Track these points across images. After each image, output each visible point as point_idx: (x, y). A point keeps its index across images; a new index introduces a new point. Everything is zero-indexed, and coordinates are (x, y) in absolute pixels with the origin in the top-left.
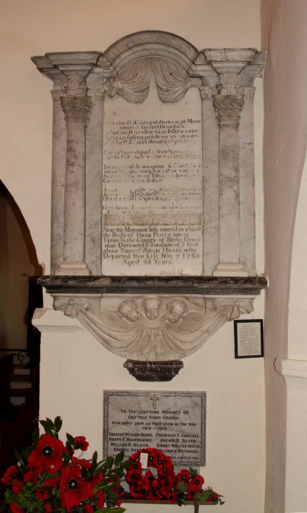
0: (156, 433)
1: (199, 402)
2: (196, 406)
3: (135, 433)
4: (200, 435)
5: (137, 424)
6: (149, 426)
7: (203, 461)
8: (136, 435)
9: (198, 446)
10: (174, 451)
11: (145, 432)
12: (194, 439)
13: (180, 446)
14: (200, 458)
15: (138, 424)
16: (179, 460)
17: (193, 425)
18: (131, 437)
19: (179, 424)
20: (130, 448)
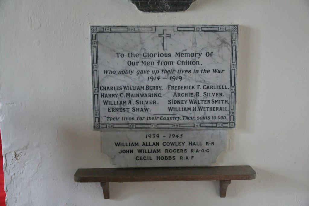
0: (167, 85)
1: (229, 40)
2: (223, 45)
3: (137, 86)
4: (228, 87)
5: (140, 72)
6: (157, 75)
7: (232, 121)
8: (139, 88)
9: (226, 102)
10: (192, 109)
11: (152, 84)
12: (220, 91)
13: (200, 102)
14: (228, 117)
15: (142, 72)
16: (200, 121)
17: (219, 72)
18: (131, 92)
19: (200, 72)
20: (130, 106)
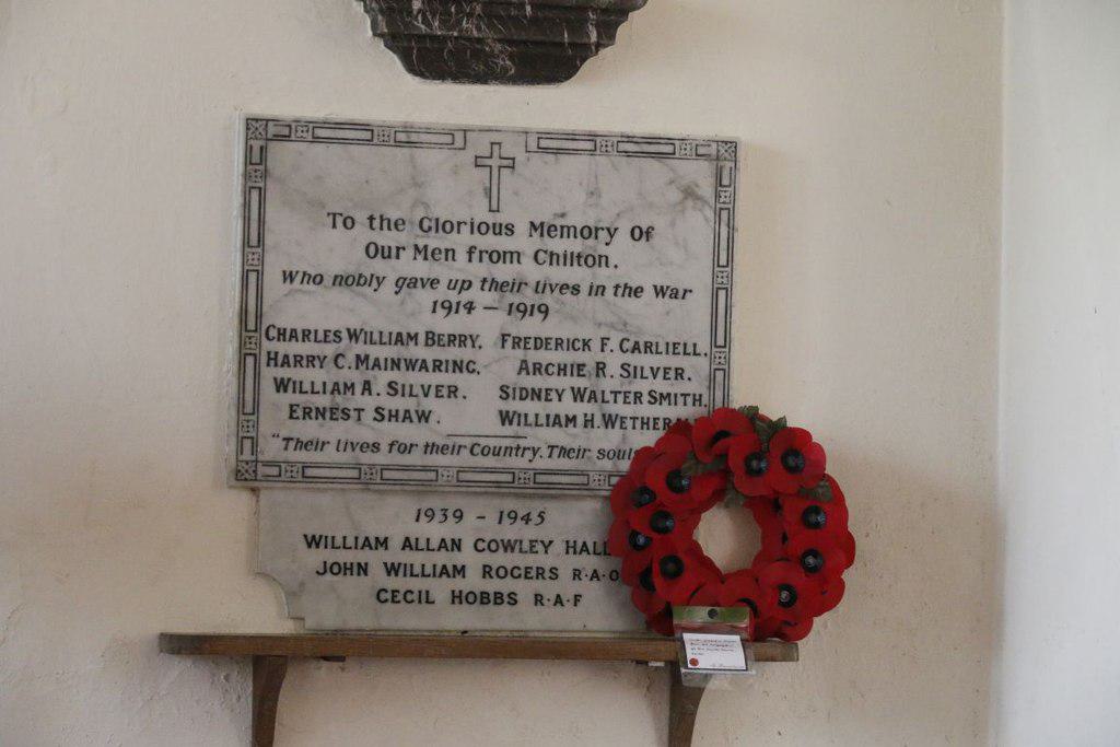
0: (497, 334)
2: (690, 203)
3: (395, 330)
4: (704, 347)
5: (406, 283)
6: (466, 296)
10: (580, 420)
11: (445, 325)
13: (609, 397)
15: (413, 283)
17: (675, 295)
18: (376, 352)
19: (610, 291)
